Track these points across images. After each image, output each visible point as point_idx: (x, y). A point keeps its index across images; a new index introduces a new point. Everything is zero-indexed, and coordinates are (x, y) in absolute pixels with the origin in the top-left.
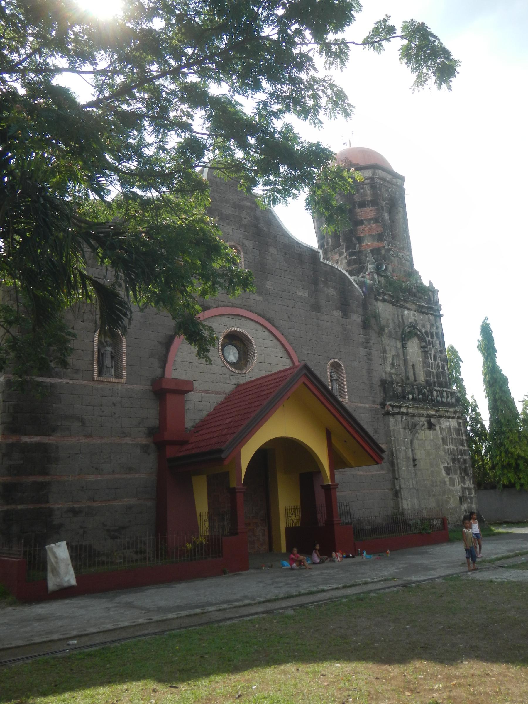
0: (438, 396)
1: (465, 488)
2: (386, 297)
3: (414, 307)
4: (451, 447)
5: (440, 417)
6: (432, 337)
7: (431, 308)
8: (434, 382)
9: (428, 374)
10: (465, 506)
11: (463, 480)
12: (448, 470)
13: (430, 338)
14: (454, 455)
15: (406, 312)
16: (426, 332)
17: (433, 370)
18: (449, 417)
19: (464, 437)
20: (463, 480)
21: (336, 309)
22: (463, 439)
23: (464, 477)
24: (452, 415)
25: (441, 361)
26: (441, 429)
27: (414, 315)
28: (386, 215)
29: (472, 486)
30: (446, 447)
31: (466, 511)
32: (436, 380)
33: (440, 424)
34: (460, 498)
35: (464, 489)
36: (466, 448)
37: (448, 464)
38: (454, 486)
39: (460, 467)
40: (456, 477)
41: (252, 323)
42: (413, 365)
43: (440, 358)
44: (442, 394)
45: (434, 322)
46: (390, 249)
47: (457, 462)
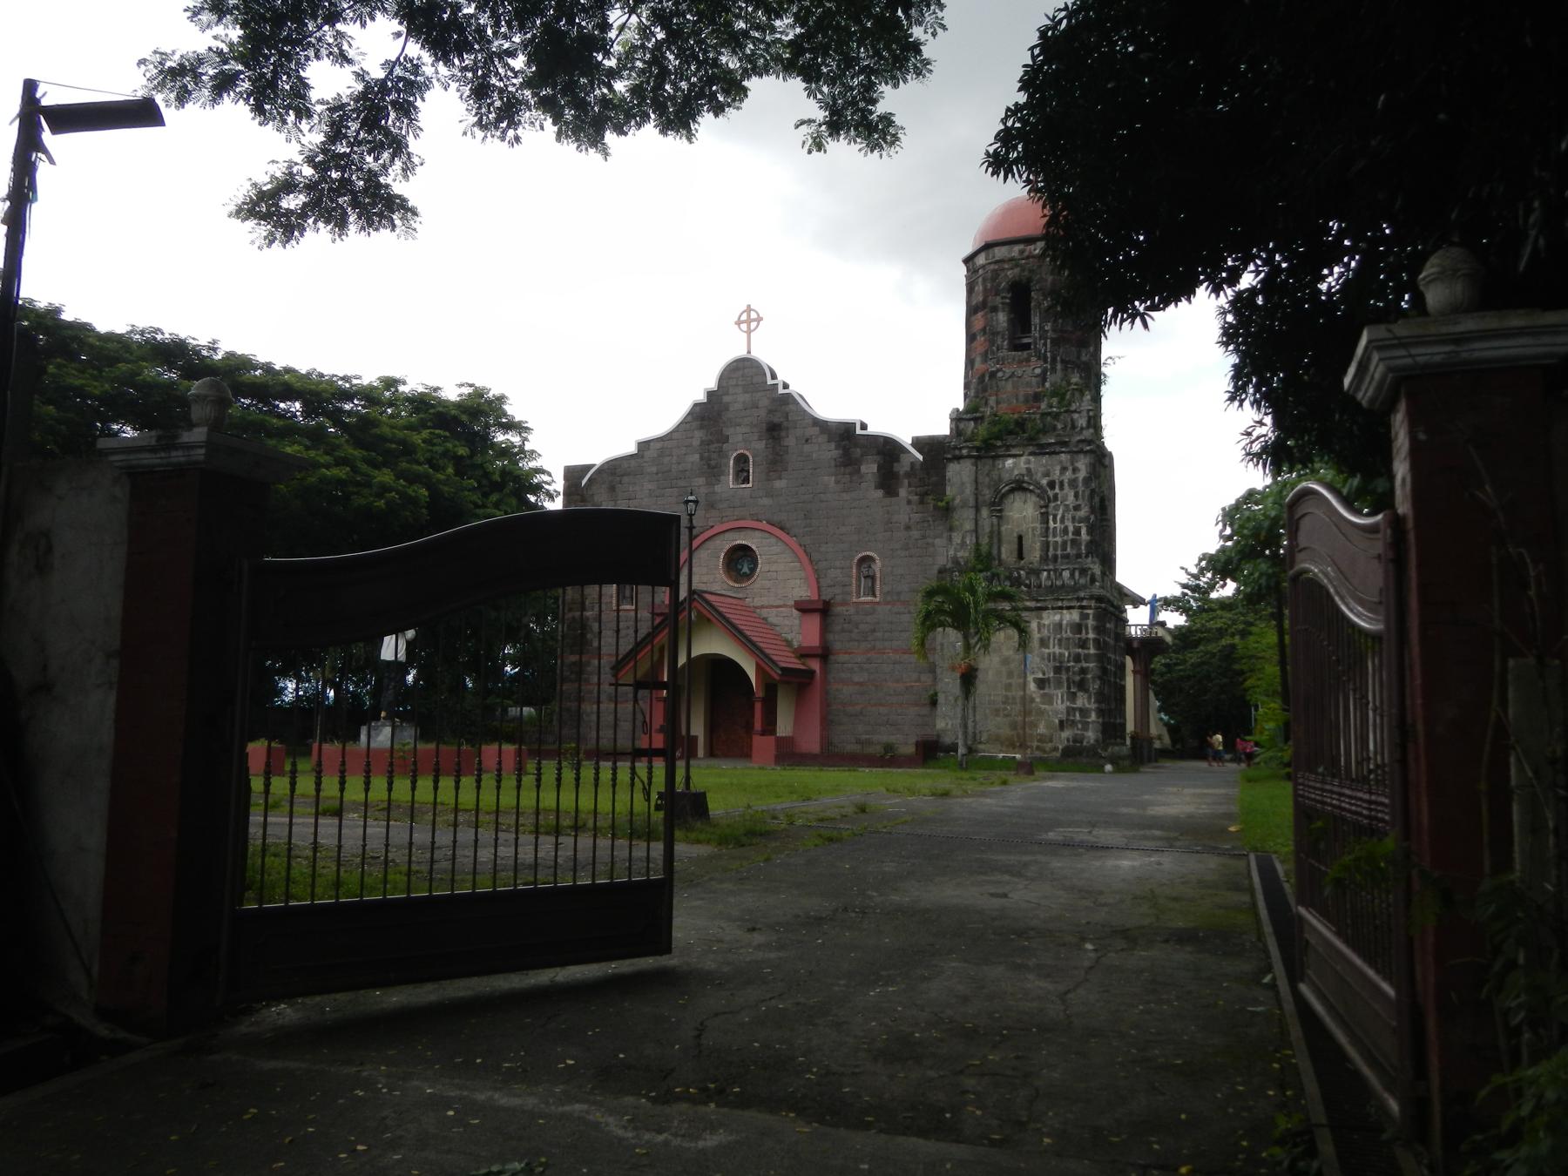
0: (1049, 577)
2: (965, 452)
3: (1031, 449)
4: (1057, 650)
5: (1046, 609)
6: (1062, 488)
7: (1065, 444)
8: (1055, 557)
9: (1046, 545)
10: (1066, 734)
11: (1072, 697)
12: (1041, 683)
15: (1010, 462)
16: (1052, 485)
17: (1058, 539)
19: (1091, 635)
20: (1072, 697)
21: (877, 488)
23: (1074, 694)
24: (1074, 603)
26: (1040, 627)
27: (1028, 462)
28: (1002, 318)
29: (1093, 706)
34: (1061, 722)
35: (1070, 711)
36: (1092, 651)
40: (1059, 694)
41: (757, 534)
42: (1020, 538)
43: (1073, 518)
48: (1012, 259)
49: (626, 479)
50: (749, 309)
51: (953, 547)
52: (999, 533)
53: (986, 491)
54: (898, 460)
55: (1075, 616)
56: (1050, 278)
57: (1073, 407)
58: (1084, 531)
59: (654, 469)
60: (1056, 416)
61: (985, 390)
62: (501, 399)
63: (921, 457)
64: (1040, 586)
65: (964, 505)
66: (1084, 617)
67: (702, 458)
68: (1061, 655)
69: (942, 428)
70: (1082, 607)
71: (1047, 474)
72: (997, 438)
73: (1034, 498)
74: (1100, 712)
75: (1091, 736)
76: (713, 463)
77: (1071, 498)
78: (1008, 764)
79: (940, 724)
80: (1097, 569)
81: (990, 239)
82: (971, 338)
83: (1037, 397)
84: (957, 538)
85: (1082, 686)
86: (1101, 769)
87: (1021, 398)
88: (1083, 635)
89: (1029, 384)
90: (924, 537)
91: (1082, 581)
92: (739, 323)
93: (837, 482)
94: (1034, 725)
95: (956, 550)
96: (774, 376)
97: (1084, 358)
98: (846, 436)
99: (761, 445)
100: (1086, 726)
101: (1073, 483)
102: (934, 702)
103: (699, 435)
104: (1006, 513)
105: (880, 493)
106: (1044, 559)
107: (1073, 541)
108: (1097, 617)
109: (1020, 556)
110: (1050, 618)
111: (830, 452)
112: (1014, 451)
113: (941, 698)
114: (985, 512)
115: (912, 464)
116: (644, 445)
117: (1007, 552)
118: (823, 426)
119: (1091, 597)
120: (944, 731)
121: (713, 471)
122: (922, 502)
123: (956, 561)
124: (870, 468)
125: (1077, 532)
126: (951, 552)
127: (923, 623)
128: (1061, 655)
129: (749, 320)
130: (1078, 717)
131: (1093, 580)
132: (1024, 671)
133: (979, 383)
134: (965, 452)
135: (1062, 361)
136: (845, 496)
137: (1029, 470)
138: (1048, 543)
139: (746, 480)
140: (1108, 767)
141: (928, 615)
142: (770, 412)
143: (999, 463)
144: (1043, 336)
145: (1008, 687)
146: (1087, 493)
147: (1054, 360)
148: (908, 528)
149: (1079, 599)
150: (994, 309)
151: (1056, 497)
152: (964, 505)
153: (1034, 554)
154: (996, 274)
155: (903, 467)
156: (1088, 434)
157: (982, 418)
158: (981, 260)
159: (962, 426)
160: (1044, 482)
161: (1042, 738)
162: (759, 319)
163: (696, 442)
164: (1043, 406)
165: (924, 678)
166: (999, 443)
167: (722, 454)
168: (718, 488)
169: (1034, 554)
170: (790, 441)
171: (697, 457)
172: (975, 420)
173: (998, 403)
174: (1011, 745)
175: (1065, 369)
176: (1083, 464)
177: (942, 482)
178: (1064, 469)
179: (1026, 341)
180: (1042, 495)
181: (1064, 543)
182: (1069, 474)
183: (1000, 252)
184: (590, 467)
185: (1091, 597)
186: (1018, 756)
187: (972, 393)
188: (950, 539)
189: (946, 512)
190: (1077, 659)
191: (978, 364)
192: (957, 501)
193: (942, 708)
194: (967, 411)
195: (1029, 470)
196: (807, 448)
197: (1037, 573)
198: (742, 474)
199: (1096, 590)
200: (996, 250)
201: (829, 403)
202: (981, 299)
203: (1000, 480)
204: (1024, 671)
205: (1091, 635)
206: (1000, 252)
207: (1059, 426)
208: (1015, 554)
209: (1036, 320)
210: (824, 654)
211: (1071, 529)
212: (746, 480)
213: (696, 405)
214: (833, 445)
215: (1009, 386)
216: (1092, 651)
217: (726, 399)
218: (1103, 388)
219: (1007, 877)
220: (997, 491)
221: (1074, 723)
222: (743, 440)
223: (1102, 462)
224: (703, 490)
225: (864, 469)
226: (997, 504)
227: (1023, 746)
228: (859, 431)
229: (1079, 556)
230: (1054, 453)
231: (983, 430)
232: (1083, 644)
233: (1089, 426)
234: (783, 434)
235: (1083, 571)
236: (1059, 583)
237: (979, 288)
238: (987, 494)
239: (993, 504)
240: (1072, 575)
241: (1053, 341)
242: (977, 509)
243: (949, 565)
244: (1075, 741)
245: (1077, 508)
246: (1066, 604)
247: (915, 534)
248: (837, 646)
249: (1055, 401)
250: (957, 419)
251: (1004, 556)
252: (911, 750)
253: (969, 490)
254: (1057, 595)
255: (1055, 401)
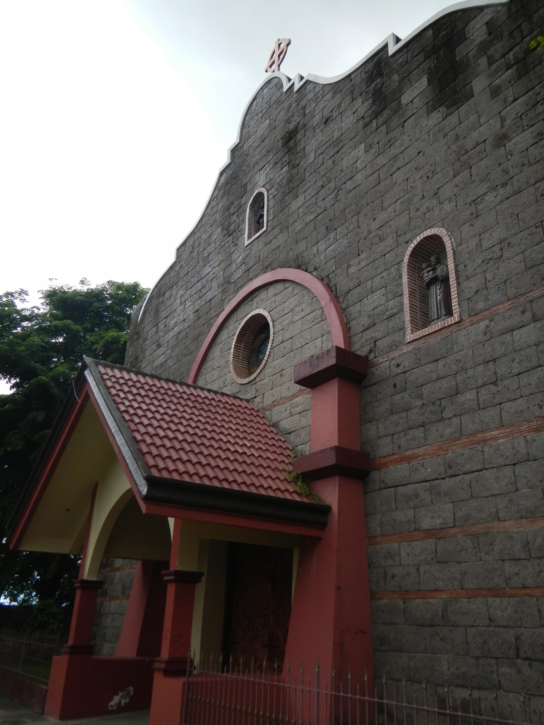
142: (288, 121)
210: (353, 465)
213: (221, 174)
248: (385, 448)
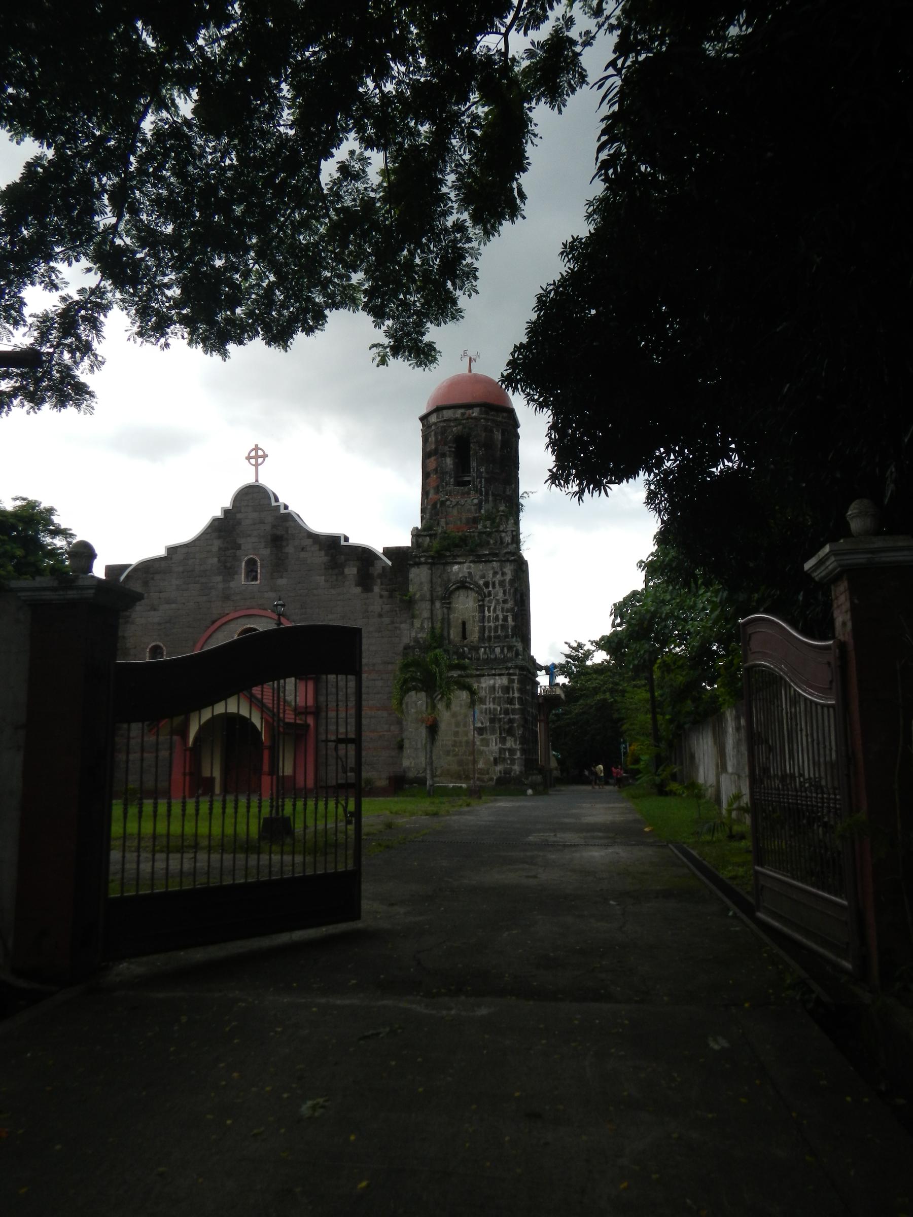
0: (485, 652)
1: (505, 750)
2: (423, 559)
3: (471, 558)
4: (492, 706)
5: (483, 675)
6: (494, 587)
8: (490, 637)
9: (483, 629)
10: (499, 768)
11: (503, 740)
13: (490, 589)
14: (494, 715)
15: (456, 567)
16: (486, 584)
17: (492, 624)
18: (495, 675)
19: (516, 695)
20: (503, 740)
21: (357, 585)
22: (514, 698)
23: (505, 738)
25: (502, 611)
27: (469, 568)
28: (449, 461)
29: (518, 747)
30: (484, 707)
31: (500, 772)
32: (492, 634)
33: (480, 683)
34: (495, 759)
35: (502, 751)
36: (517, 706)
37: (482, 723)
38: (488, 746)
39: (500, 727)
40: (493, 738)
41: (264, 620)
42: (464, 624)
43: (503, 609)
44: (494, 650)
45: (498, 570)
46: (447, 500)
47: (497, 722)
48: (456, 419)
49: (157, 577)
50: (257, 448)
51: (415, 630)
52: (449, 619)
53: (439, 589)
54: (372, 564)
55: (504, 681)
56: (484, 435)
57: (501, 528)
58: (510, 619)
59: (181, 569)
60: (489, 534)
61: (437, 514)
62: (50, 511)
63: (390, 563)
64: (478, 659)
65: (423, 599)
66: (511, 681)
67: (219, 561)
68: (495, 709)
69: (406, 541)
70: (509, 674)
71: (483, 577)
72: (447, 550)
73: (472, 595)
74: (523, 751)
75: (517, 768)
76: (229, 565)
77: (501, 594)
78: (457, 792)
79: (406, 763)
80: (520, 646)
81: (440, 404)
82: (426, 475)
83: (475, 521)
84: (417, 623)
85: (510, 732)
86: (524, 793)
87: (464, 521)
88: (511, 695)
89: (469, 511)
90: (393, 622)
91: (509, 655)
92: (249, 458)
93: (326, 581)
94: (475, 762)
95: (417, 633)
96: (277, 500)
97: (508, 493)
98: (333, 545)
99: (266, 552)
100: (513, 761)
101: (502, 583)
102: (401, 747)
103: (217, 544)
104: (453, 605)
105: (358, 590)
106: (482, 639)
107: (502, 625)
108: (519, 681)
109: (464, 637)
110: (486, 683)
111: (319, 558)
112: (459, 560)
113: (406, 744)
114: (438, 604)
115: (383, 567)
116: (172, 550)
117: (454, 634)
118: (316, 538)
119: (516, 667)
120: (409, 768)
121: (228, 570)
122: (391, 596)
123: (416, 640)
124: (351, 571)
125: (505, 619)
126: (413, 634)
127: (401, 688)
128: (495, 709)
129: (257, 456)
130: (507, 755)
131: (517, 654)
132: (468, 722)
133: (431, 507)
134: (423, 559)
135: (493, 495)
136: (333, 591)
137: (470, 573)
138: (484, 627)
139: (255, 579)
140: (530, 792)
141: (405, 681)
142: (274, 527)
143: (448, 569)
144: (479, 476)
145: (456, 734)
146: (512, 591)
147: (487, 494)
148: (380, 616)
149: (508, 668)
150: (444, 455)
151: (490, 593)
152: (423, 599)
153: (474, 636)
154: (444, 431)
155: (377, 570)
156: (512, 548)
157: (435, 535)
158: (433, 419)
159: (420, 540)
160: (481, 582)
161: (481, 771)
162: (265, 456)
163: (215, 549)
164: (480, 527)
165: (392, 728)
166: (448, 554)
167: (237, 559)
168: (232, 584)
169: (474, 636)
170: (290, 549)
171: (216, 560)
172: (430, 536)
173: (447, 524)
174: (459, 777)
175: (495, 501)
176: (509, 569)
177: (406, 581)
178: (495, 573)
179: (466, 479)
180: (479, 591)
181: (496, 627)
182: (499, 577)
183: (447, 414)
184: (126, 567)
185: (516, 667)
186: (464, 785)
187: (427, 516)
188: (412, 624)
189: (409, 604)
190: (506, 712)
191: (432, 495)
192: (417, 596)
193: (407, 751)
194: (425, 528)
195: (470, 573)
196: (303, 555)
197: (477, 649)
198: (251, 573)
199: (520, 662)
200: (445, 412)
201: (319, 519)
202: (433, 447)
203: (449, 580)
204: (468, 722)
205: (516, 695)
206: (447, 414)
207: (492, 542)
208: (461, 634)
209: (474, 464)
210: (317, 712)
211: (501, 617)
212: (255, 579)
214: (323, 553)
215: (455, 512)
216: (517, 706)
217: (239, 516)
218: (521, 514)
219: (527, 866)
220: (447, 589)
221: (504, 760)
222: (253, 548)
223: (521, 567)
224: (220, 586)
225: (347, 571)
226: (447, 598)
227: (467, 778)
228: (343, 543)
229: (506, 636)
230: (491, 562)
231: (436, 544)
232: (511, 701)
233: (512, 543)
234: (284, 544)
235: (510, 648)
236: (492, 657)
237: (432, 439)
238: (440, 591)
239: (444, 598)
240: (502, 650)
241: (486, 480)
242: (432, 602)
243: (412, 644)
244: (505, 773)
245: (505, 602)
246: (498, 672)
247: (386, 620)
249: (488, 523)
250: (417, 534)
251: (452, 637)
252: (383, 783)
253: (426, 588)
254: (492, 665)
255: (488, 523)
